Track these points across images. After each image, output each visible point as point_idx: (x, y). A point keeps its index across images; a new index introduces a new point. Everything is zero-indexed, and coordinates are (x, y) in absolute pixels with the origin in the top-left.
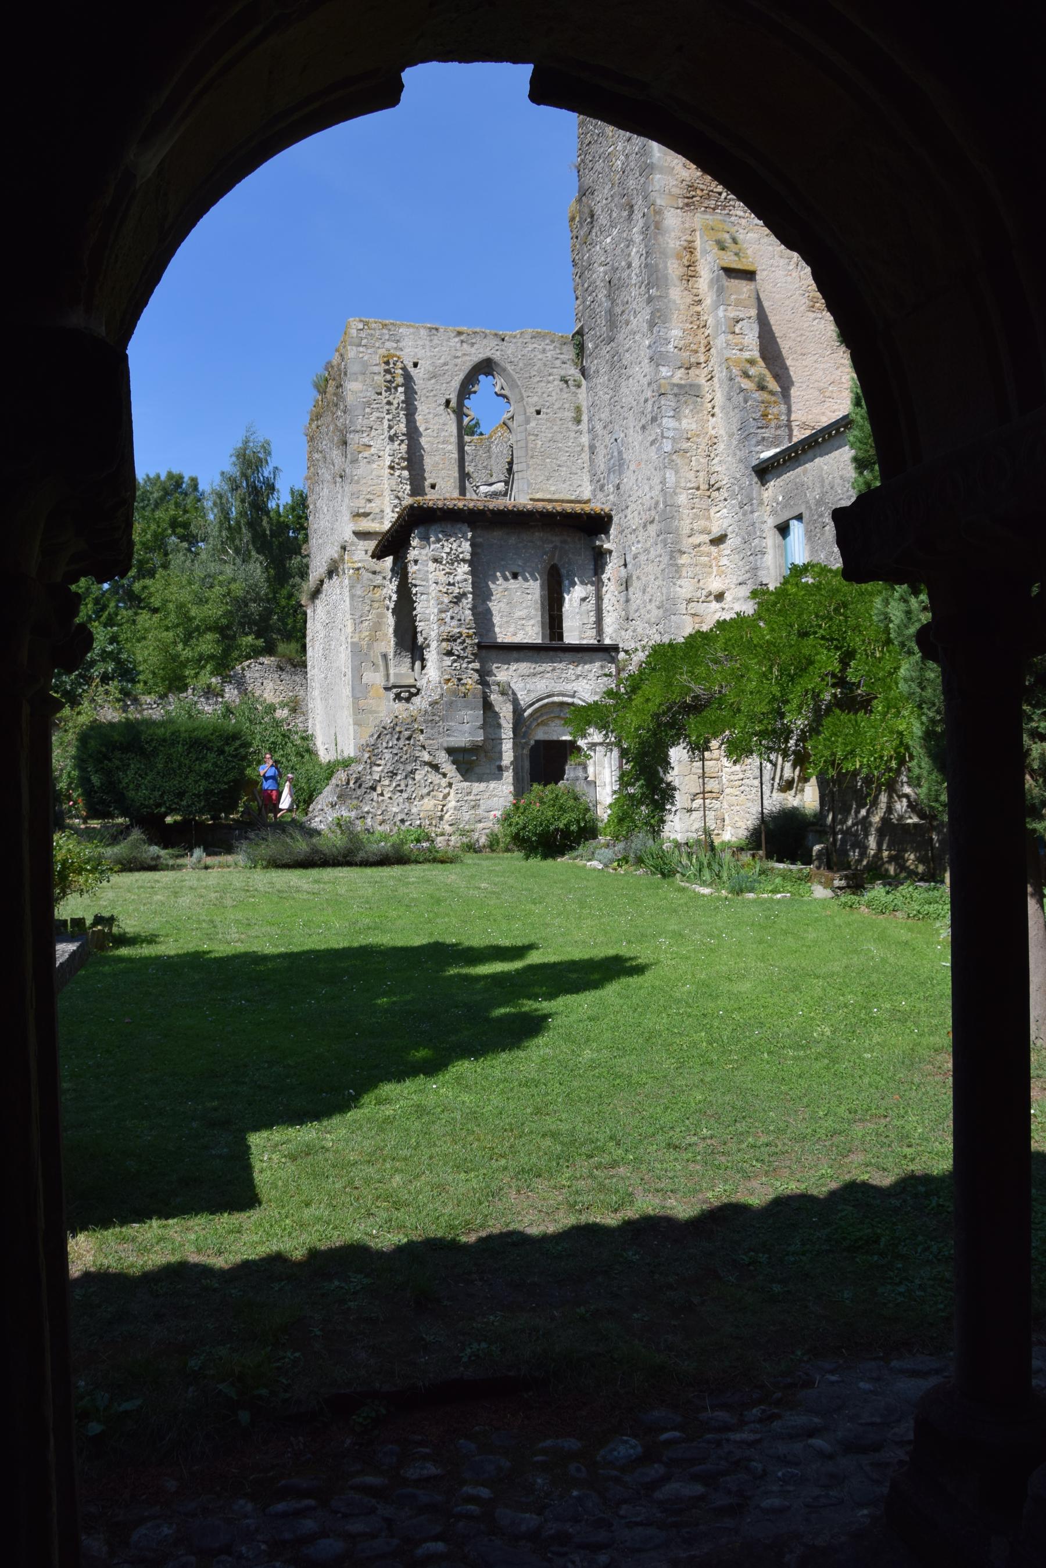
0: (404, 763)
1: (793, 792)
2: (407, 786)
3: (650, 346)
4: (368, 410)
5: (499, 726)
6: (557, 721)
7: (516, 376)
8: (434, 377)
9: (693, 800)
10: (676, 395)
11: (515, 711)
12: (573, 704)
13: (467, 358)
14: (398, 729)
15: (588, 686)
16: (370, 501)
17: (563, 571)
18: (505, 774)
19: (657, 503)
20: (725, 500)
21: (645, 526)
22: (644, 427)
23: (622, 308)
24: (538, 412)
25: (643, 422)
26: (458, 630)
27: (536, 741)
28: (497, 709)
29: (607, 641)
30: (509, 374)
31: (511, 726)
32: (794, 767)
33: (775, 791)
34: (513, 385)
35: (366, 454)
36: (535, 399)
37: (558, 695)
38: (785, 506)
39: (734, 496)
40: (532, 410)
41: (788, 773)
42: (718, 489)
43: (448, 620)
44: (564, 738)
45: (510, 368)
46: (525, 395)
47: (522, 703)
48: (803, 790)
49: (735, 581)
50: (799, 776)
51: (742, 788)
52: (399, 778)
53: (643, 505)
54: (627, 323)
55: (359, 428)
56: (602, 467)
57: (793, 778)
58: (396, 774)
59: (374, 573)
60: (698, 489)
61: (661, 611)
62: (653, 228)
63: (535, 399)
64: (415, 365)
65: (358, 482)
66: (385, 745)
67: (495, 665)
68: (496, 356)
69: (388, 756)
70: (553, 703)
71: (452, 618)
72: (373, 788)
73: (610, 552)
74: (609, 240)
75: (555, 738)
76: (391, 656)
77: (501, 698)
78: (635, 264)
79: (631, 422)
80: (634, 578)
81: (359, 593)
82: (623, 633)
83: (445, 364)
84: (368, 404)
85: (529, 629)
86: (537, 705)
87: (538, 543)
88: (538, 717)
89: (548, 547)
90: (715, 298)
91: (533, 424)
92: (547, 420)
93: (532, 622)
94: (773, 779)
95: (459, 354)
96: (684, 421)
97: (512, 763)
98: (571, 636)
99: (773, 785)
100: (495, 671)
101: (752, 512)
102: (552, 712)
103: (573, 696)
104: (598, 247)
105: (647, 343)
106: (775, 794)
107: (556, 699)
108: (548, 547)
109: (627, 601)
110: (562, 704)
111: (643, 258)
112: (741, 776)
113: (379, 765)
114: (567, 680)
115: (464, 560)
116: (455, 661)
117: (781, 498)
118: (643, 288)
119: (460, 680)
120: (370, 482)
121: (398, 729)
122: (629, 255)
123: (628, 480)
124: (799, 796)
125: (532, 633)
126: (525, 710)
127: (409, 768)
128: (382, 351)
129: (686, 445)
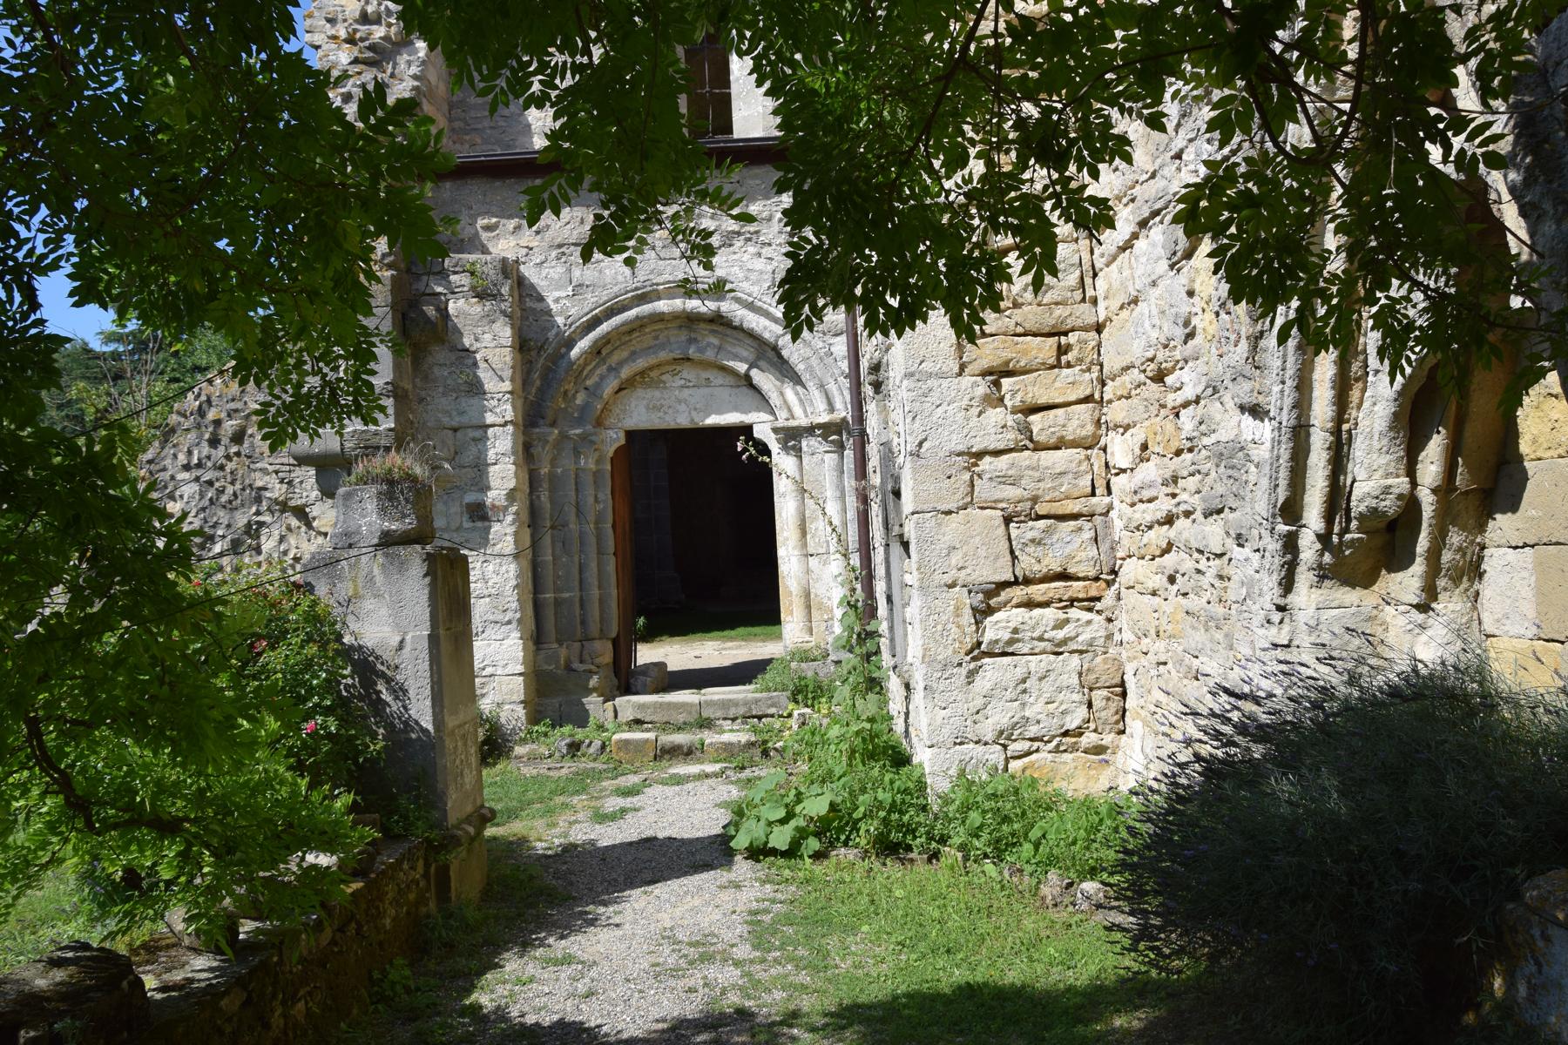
0: (230, 507)
1: (1407, 583)
2: (237, 570)
5: (475, 389)
6: (688, 373)
9: (982, 613)
11: (524, 346)
12: (719, 321)
14: (211, 415)
15: (759, 264)
18: (496, 528)
27: (630, 434)
28: (467, 341)
31: (507, 386)
32: (1412, 426)
33: (1304, 577)
41: (1374, 476)
44: (713, 420)
47: (560, 320)
48: (1474, 570)
50: (1444, 490)
51: (1169, 560)
57: (1411, 504)
66: (182, 458)
67: (481, 222)
69: (189, 490)
70: (658, 318)
75: (683, 421)
77: (475, 308)
88: (621, 364)
94: (1291, 510)
97: (511, 495)
99: (1290, 545)
100: (484, 235)
102: (662, 347)
106: (1305, 595)
107: (663, 306)
110: (690, 320)
112: (1164, 506)
121: (211, 415)
124: (1450, 605)
126: (570, 343)
127: (241, 520)
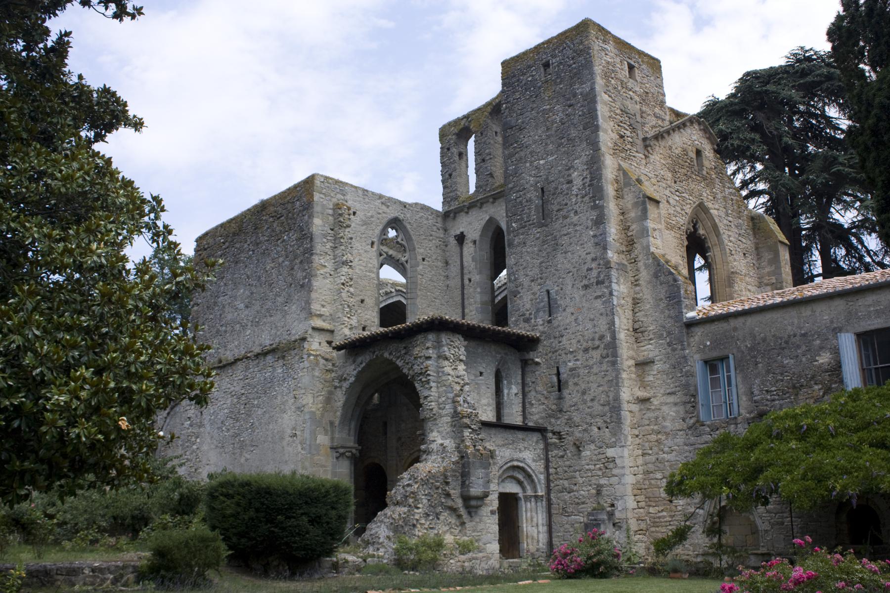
3: (595, 236)
4: (325, 240)
7: (412, 233)
8: (365, 224)
10: (617, 269)
13: (384, 215)
16: (323, 306)
17: (504, 374)
19: (602, 338)
20: (651, 339)
21: (586, 350)
22: (586, 287)
23: (558, 207)
24: (424, 259)
25: (585, 282)
26: (469, 410)
29: (531, 424)
30: (407, 231)
34: (408, 238)
35: (322, 271)
36: (422, 250)
37: (517, 460)
38: (711, 348)
39: (660, 337)
40: (420, 258)
42: (642, 332)
43: (462, 402)
45: (408, 227)
46: (417, 246)
49: (662, 391)
52: (431, 518)
53: (583, 336)
54: (565, 217)
55: (318, 252)
56: (528, 306)
58: (428, 515)
59: (327, 360)
60: (628, 330)
61: (607, 408)
62: (594, 165)
63: (422, 250)
64: (354, 213)
65: (316, 291)
68: (401, 217)
69: (425, 501)
71: (464, 401)
72: (414, 526)
73: (538, 364)
74: (542, 162)
76: (337, 423)
78: (578, 182)
79: (569, 281)
80: (570, 383)
81: (317, 374)
82: (553, 420)
83: (372, 217)
84: (325, 236)
85: (488, 412)
86: (505, 467)
87: (494, 353)
89: (499, 356)
90: (639, 213)
91: (421, 267)
92: (429, 266)
93: (491, 408)
95: (380, 211)
96: (622, 286)
98: (507, 420)
101: (683, 349)
103: (521, 462)
104: (528, 165)
105: (592, 233)
108: (499, 356)
109: (560, 398)
110: (518, 467)
111: (588, 180)
113: (418, 508)
114: (520, 451)
115: (461, 360)
116: (470, 433)
117: (708, 343)
118: (587, 198)
119: (475, 446)
120: (324, 293)
122: (570, 175)
123: (562, 318)
125: (488, 415)
128: (334, 200)
129: (623, 302)
